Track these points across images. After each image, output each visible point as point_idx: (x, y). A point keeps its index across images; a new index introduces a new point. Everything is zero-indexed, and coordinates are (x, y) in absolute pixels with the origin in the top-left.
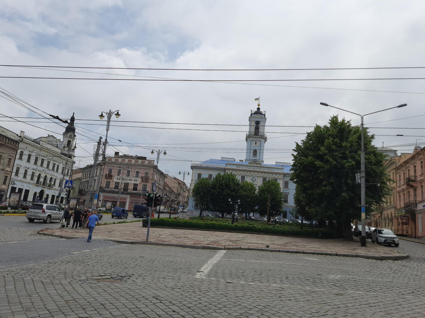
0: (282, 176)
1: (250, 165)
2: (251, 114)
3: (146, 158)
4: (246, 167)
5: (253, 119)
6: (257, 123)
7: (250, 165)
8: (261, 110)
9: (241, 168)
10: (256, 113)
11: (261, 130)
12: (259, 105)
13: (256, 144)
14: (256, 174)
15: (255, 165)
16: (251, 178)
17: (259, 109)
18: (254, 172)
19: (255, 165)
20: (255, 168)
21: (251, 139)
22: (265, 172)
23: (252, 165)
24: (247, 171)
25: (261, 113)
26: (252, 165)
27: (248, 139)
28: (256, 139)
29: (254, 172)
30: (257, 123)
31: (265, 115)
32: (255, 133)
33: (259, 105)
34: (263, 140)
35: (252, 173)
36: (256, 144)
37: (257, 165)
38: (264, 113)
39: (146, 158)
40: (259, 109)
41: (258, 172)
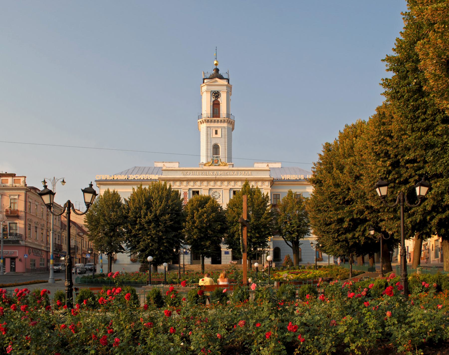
1: (205, 168)
3: (15, 175)
6: (216, 95)
13: (216, 133)
18: (216, 180)
24: (202, 180)
28: (216, 125)
29: (216, 180)
30: (216, 95)
31: (228, 80)
35: (212, 183)
36: (216, 133)
39: (15, 175)
41: (223, 180)
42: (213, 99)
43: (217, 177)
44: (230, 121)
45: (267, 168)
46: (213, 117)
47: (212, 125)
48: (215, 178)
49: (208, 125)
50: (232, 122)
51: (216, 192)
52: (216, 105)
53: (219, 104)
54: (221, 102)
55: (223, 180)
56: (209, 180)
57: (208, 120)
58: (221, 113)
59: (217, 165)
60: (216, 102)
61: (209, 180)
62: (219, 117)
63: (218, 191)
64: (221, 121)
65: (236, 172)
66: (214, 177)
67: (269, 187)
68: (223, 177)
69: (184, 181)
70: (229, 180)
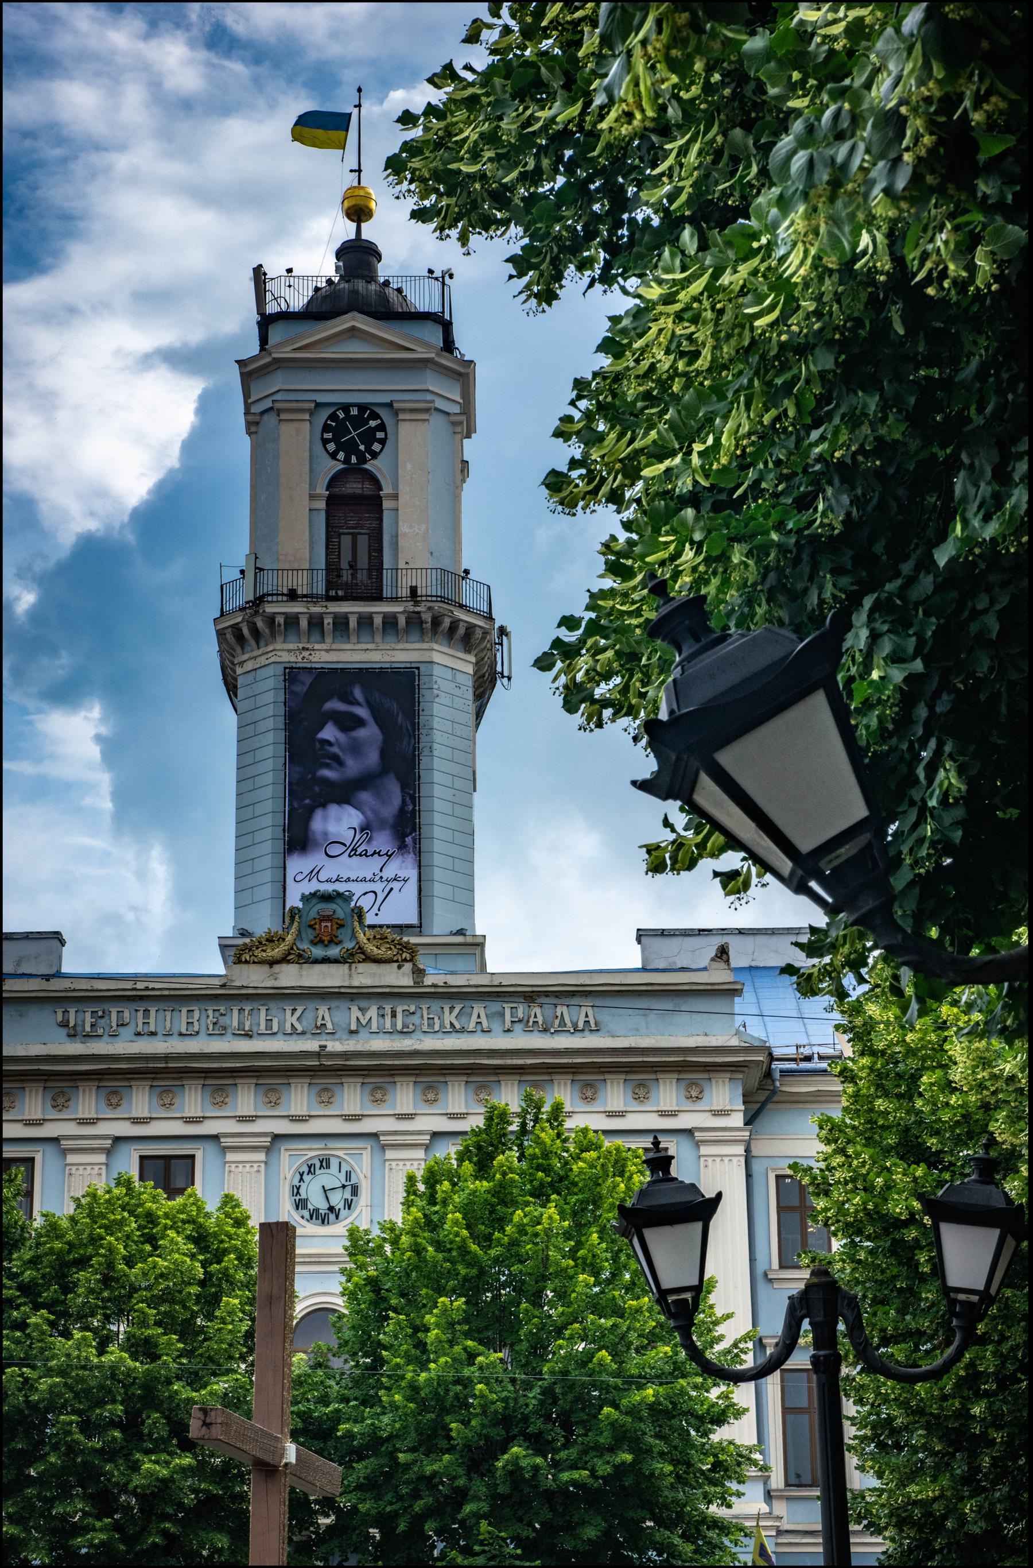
0: (725, 1096)
1: (255, 977)
2: (266, 322)
4: (202, 1017)
6: (355, 434)
7: (255, 977)
8: (384, 270)
9: (125, 1045)
10: (326, 305)
14: (352, 1098)
15: (331, 977)
16: (289, 1163)
18: (325, 1072)
19: (331, 977)
23: (290, 976)
25: (388, 309)
26: (290, 976)
27: (249, 661)
32: (332, 569)
35: (299, 1099)
37: (366, 976)
38: (423, 298)
43: (334, 1046)
44: (454, 625)
45: (720, 976)
48: (318, 1055)
50: (471, 628)
51: (325, 1163)
52: (356, 508)
54: (387, 490)
55: (379, 1072)
56: (271, 1074)
57: (292, 621)
59: (334, 951)
60: (354, 487)
63: (339, 1150)
64: (390, 622)
65: (478, 1008)
66: (311, 1045)
67: (737, 1120)
69: (76, 1078)
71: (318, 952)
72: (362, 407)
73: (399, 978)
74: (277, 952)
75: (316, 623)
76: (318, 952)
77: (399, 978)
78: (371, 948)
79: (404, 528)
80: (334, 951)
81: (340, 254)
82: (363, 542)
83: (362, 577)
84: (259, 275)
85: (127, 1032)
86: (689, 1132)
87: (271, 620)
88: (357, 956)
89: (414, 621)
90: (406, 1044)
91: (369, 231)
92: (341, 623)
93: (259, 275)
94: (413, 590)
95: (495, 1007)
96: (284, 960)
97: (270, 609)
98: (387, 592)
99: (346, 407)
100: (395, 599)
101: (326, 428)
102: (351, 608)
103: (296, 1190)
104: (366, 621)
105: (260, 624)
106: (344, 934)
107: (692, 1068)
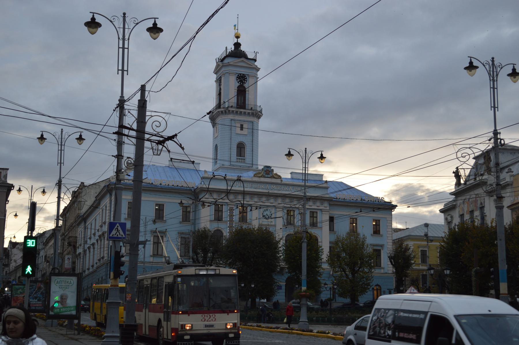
0: (326, 204)
1: (256, 179)
5: (230, 68)
6: (242, 78)
7: (256, 179)
8: (242, 48)
11: (249, 96)
12: (238, 37)
13: (242, 128)
16: (262, 210)
17: (237, 45)
20: (268, 186)
21: (231, 116)
22: (291, 197)
23: (262, 179)
26: (262, 179)
29: (269, 195)
30: (242, 78)
33: (238, 37)
34: (254, 119)
36: (242, 128)
38: (250, 56)
40: (237, 45)
41: (276, 196)
42: (238, 84)
43: (270, 192)
46: (237, 108)
47: (237, 117)
49: (232, 118)
51: (267, 210)
52: (242, 92)
53: (245, 91)
57: (233, 111)
58: (247, 103)
59: (269, 176)
60: (241, 89)
61: (260, 195)
62: (245, 108)
64: (249, 113)
65: (291, 187)
66: (267, 191)
67: (328, 208)
68: (276, 192)
70: (284, 196)
71: (267, 176)
72: (243, 75)
73: (278, 181)
74: (260, 175)
75: (237, 112)
76: (267, 176)
77: (278, 181)
78: (275, 176)
79: (250, 97)
80: (269, 176)
81: (234, 45)
82: (242, 98)
83: (242, 104)
84: (226, 48)
85: (237, 186)
86: (321, 210)
87: (229, 111)
88: (273, 177)
89: (253, 114)
90: (280, 192)
91: (240, 41)
92: (241, 112)
93: (226, 48)
94: (252, 108)
95: (293, 187)
96: (261, 177)
97: (230, 109)
98: (247, 108)
99: (241, 74)
100: (248, 109)
101: (237, 77)
102: (242, 110)
103: (263, 214)
104: (245, 113)
105: (227, 111)
106: (270, 173)
107: (322, 199)
